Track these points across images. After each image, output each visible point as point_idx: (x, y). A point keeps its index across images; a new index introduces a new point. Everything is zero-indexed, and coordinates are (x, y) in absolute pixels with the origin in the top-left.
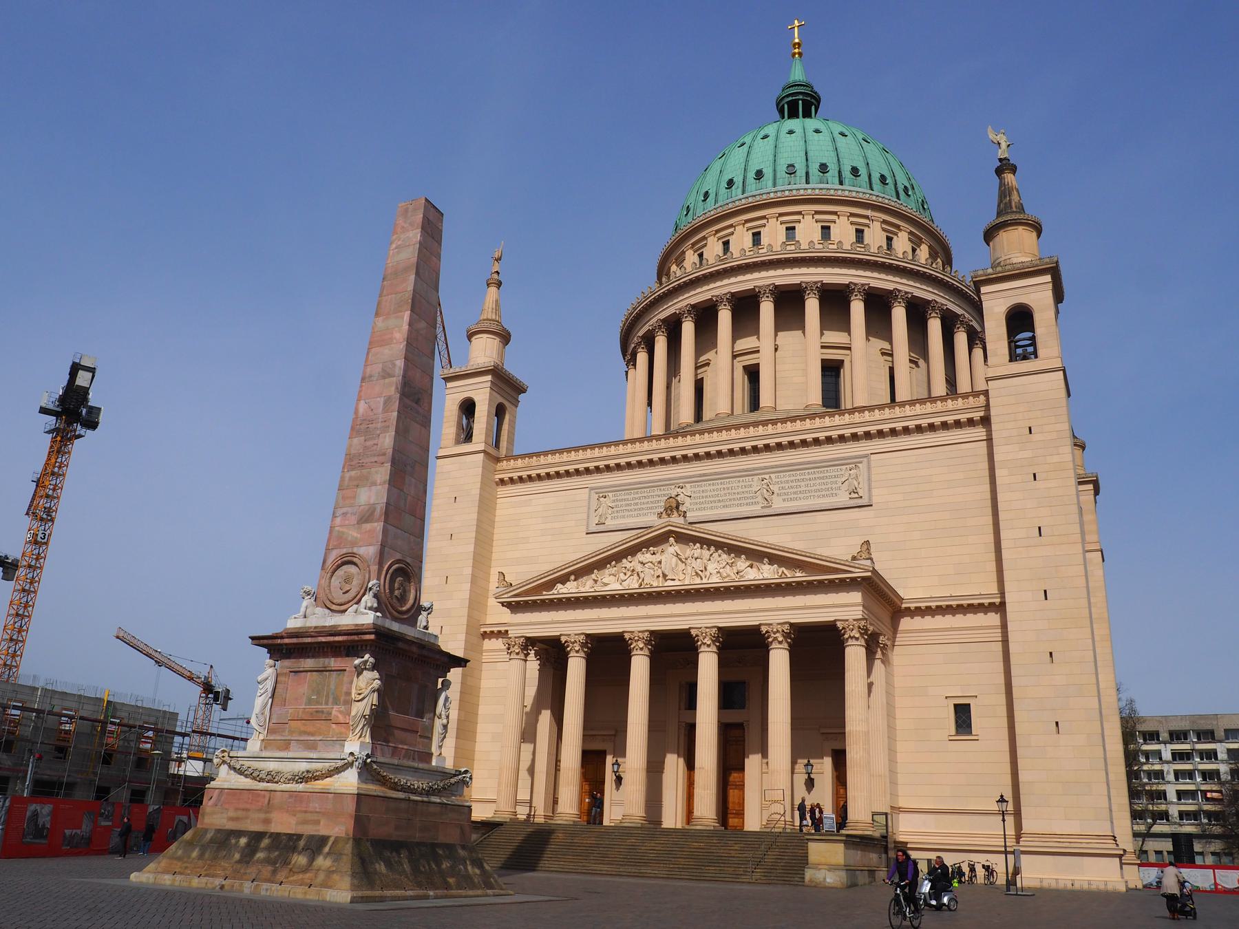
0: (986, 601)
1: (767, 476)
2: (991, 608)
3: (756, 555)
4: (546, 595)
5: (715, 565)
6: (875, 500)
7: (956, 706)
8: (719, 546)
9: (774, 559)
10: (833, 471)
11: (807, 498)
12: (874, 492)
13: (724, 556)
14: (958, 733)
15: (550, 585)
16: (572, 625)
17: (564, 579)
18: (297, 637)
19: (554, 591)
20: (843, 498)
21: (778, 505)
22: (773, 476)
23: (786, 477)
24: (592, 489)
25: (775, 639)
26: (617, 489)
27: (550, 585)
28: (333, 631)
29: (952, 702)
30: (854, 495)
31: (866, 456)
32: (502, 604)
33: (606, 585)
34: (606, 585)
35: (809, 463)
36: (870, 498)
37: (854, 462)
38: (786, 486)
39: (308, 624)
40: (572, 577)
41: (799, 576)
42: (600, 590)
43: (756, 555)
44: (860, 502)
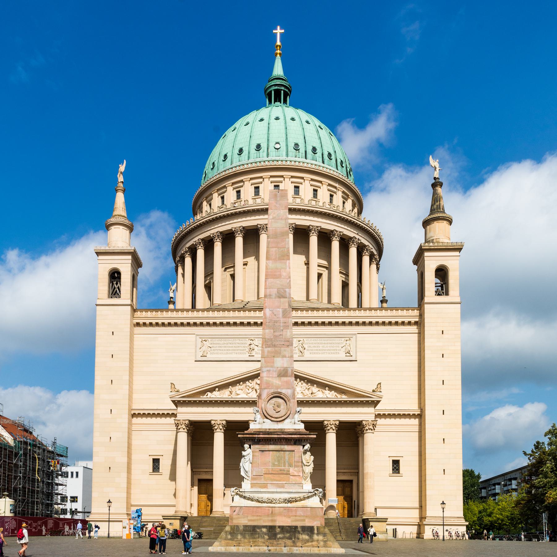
0: (411, 413)
1: (302, 339)
2: (414, 416)
3: (322, 385)
4: (203, 398)
5: (300, 389)
8: (302, 379)
9: (332, 388)
10: (337, 340)
11: (323, 353)
13: (304, 384)
15: (204, 392)
16: (218, 416)
17: (212, 390)
18: (268, 434)
19: (205, 397)
20: (342, 356)
21: (307, 355)
22: (305, 339)
23: (312, 341)
24: (197, 335)
25: (331, 428)
26: (213, 337)
27: (204, 392)
28: (282, 432)
30: (349, 355)
31: (355, 334)
32: (173, 401)
33: (238, 395)
34: (238, 395)
35: (325, 334)
38: (312, 345)
39: (264, 427)
40: (217, 389)
41: (344, 398)
42: (234, 397)
43: (322, 385)
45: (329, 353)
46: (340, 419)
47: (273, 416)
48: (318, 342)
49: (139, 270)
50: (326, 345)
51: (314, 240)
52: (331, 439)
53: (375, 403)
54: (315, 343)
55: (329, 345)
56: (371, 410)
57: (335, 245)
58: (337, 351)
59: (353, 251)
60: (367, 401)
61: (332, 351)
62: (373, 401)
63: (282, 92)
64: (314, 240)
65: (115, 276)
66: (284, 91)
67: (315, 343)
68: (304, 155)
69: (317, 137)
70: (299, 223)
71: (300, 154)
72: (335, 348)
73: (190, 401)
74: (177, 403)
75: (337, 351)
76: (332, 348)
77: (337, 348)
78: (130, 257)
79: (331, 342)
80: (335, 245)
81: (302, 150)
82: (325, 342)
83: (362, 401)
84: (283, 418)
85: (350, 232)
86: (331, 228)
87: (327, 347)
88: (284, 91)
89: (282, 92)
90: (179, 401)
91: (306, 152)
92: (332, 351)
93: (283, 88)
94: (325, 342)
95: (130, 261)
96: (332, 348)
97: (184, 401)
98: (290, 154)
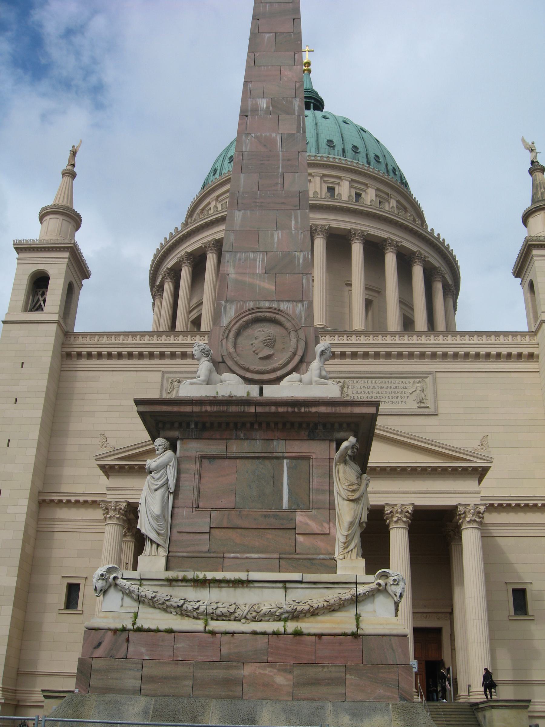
1: (342, 380)
6: (441, 411)
7: (514, 590)
12: (440, 404)
14: (516, 614)
20: (412, 406)
22: (347, 380)
24: (164, 373)
29: (510, 588)
31: (430, 373)
32: (102, 467)
36: (436, 407)
37: (421, 376)
38: (359, 390)
44: (427, 411)
45: (389, 403)
46: (416, 503)
47: (252, 367)
48: (370, 384)
49: (85, 282)
50: (383, 390)
51: (357, 250)
52: (399, 541)
53: (480, 473)
54: (364, 387)
55: (388, 390)
56: (471, 484)
57: (391, 259)
58: (403, 400)
59: (418, 272)
60: (465, 469)
61: (393, 400)
62: (475, 469)
63: (312, 105)
64: (357, 250)
65: (39, 282)
66: (313, 103)
67: (364, 387)
68: (341, 152)
69: (358, 136)
70: (334, 224)
71: (336, 152)
72: (399, 395)
73: (132, 467)
74: (109, 470)
75: (403, 400)
76: (393, 395)
77: (403, 395)
78: (67, 254)
79: (392, 385)
80: (391, 259)
81: (339, 148)
82: (382, 385)
83: (455, 469)
84: (279, 373)
85: (411, 244)
86: (385, 235)
87: (385, 392)
88: (314, 104)
89: (312, 105)
90: (112, 467)
91: (344, 150)
92: (393, 400)
93: (313, 101)
94: (382, 385)
95: (66, 261)
96: (393, 395)
97: (122, 467)
98: (322, 150)
